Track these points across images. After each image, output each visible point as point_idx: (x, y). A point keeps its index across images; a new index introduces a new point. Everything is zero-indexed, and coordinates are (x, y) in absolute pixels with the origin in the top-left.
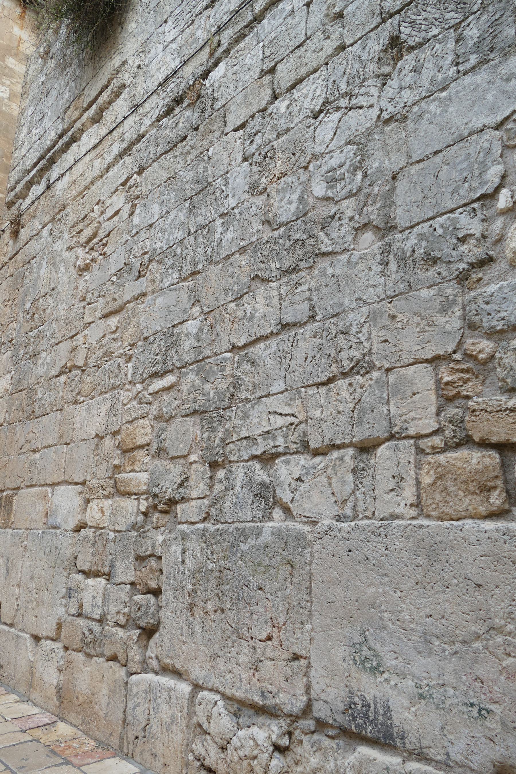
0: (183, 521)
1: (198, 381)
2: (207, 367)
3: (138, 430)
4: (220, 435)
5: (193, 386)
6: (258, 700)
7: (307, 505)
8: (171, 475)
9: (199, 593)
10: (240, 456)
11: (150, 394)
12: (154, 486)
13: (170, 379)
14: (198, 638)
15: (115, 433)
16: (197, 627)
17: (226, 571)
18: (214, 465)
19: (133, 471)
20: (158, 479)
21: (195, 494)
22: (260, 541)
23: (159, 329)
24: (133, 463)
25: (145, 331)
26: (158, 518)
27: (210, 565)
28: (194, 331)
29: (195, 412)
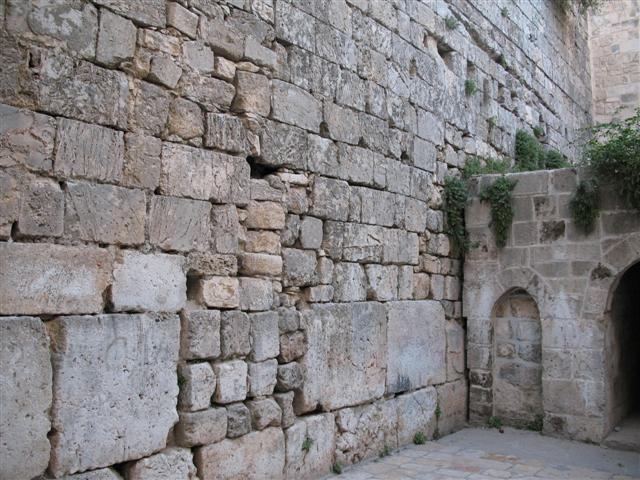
1: (328, 193)
2: (335, 185)
3: (271, 213)
4: (341, 240)
5: (324, 194)
6: (368, 398)
7: (383, 292)
8: (307, 264)
12: (292, 270)
13: (301, 178)
14: (335, 380)
15: (241, 207)
16: (335, 372)
18: (335, 261)
19: (265, 252)
21: (325, 281)
22: (368, 312)
24: (264, 245)
25: (277, 112)
28: (325, 148)
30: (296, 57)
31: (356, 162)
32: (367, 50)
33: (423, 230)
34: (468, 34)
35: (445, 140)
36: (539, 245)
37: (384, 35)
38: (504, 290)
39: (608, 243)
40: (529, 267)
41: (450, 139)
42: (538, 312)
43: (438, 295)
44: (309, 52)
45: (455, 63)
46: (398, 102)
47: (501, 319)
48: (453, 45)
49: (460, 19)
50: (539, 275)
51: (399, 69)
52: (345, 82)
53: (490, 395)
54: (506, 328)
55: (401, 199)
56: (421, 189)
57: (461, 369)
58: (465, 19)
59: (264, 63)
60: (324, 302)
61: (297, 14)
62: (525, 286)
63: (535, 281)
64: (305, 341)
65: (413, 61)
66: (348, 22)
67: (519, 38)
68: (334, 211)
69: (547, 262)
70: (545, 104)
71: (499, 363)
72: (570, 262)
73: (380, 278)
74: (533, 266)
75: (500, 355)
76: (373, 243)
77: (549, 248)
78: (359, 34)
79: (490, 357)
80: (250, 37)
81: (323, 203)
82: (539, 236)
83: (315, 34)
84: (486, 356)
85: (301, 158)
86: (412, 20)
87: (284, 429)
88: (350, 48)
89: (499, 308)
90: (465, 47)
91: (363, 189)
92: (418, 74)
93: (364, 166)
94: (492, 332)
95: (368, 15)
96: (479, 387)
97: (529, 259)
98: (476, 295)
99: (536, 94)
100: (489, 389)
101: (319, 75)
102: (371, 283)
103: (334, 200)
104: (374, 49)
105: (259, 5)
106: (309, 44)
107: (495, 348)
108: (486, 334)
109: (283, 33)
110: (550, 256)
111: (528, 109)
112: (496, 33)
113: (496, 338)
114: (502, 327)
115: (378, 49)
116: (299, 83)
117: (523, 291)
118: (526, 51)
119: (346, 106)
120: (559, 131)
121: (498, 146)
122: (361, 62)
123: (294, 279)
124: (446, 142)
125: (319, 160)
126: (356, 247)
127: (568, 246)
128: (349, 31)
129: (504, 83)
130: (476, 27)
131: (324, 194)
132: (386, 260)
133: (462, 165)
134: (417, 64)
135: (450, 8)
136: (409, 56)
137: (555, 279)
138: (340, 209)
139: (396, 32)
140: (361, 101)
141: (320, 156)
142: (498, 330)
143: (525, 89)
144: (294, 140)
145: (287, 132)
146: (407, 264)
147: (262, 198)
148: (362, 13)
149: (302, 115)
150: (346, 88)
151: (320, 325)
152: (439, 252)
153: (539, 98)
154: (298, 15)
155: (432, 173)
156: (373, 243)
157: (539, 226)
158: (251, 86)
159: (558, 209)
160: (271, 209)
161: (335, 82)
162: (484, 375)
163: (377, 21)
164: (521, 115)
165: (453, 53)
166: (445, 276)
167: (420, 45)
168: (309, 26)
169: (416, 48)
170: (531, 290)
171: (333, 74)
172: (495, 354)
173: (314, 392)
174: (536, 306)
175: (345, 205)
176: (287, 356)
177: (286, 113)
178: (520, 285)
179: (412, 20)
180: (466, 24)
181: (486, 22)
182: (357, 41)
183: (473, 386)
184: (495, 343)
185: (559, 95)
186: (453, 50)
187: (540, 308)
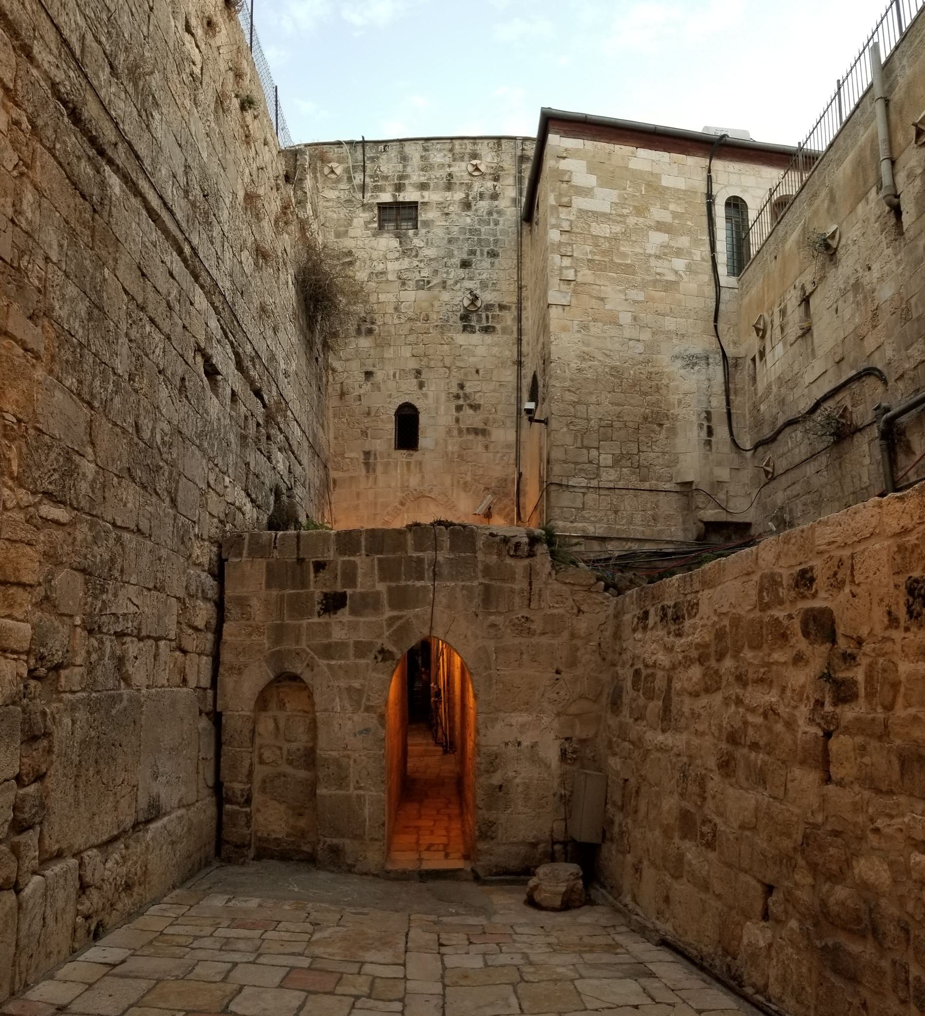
0: (67, 689)
1: (89, 538)
3: (24, 560)
5: (85, 539)
6: (115, 833)
9: (83, 763)
10: (109, 630)
11: (41, 517)
13: (60, 514)
17: (102, 736)
20: (47, 636)
23: (58, 436)
24: (11, 606)
26: (35, 687)
27: (93, 734)
28: (90, 477)
29: (83, 571)
30: (66, 347)
31: (121, 500)
32: (140, 353)
33: (182, 596)
34: (233, 357)
35: (208, 483)
36: (316, 619)
37: (157, 339)
38: (272, 677)
39: (392, 620)
40: (304, 645)
41: (212, 482)
42: (313, 704)
43: (192, 683)
44: (80, 343)
45: (220, 390)
46: (167, 428)
47: (263, 714)
48: (220, 367)
49: (227, 337)
50: (316, 657)
51: (169, 387)
52: (116, 392)
53: (249, 816)
54: (271, 725)
55: (164, 553)
56: (183, 543)
57: (211, 782)
58: (231, 338)
59: (30, 346)
60: (74, 692)
61: (70, 288)
62: (299, 672)
63: (310, 666)
64: (50, 751)
65: (183, 379)
66: (123, 314)
67: (275, 371)
68: (94, 563)
69: (326, 641)
70: (293, 453)
71: (260, 772)
72: (351, 642)
73: (136, 658)
74: (308, 646)
75: (262, 762)
76: (133, 609)
77: (327, 624)
78: (134, 334)
79: (251, 765)
80: (15, 306)
81: (84, 550)
82: (317, 608)
83: (89, 320)
84: (246, 763)
85: (64, 487)
86: (184, 327)
87: (18, 892)
88: (123, 347)
89: (262, 702)
90: (230, 371)
91: (126, 536)
92: (186, 397)
93: (130, 505)
94: (253, 731)
95: (142, 309)
96: (236, 807)
97: (304, 638)
98: (236, 682)
99: (287, 439)
100: (248, 809)
101: (89, 377)
102: (127, 664)
103: (96, 548)
104: (147, 355)
105: (29, 263)
106: (81, 331)
107: (256, 752)
108: (246, 732)
109: (53, 309)
110: (329, 635)
111: (280, 456)
112: (257, 361)
113: (258, 741)
114: (266, 726)
115: (151, 356)
116: (68, 384)
117: (295, 678)
118: (280, 388)
119: (115, 424)
120: (304, 485)
121: (254, 496)
122: (133, 369)
123: (42, 658)
124: (209, 486)
125: (83, 492)
126: (114, 614)
127: (350, 622)
128: (124, 326)
129: (261, 422)
130: (241, 351)
131: (85, 539)
132: (144, 633)
133: (222, 516)
134: (187, 383)
135: (218, 320)
136: (180, 372)
137: (333, 662)
138: (101, 562)
139: (169, 338)
140: (130, 420)
141: (84, 487)
142: (261, 728)
143: (278, 433)
144: (58, 461)
145: (50, 448)
146: (165, 639)
147: (15, 538)
148: (138, 306)
149: (69, 427)
150: (117, 400)
151: (70, 724)
152: (196, 624)
153: (290, 445)
154: (72, 290)
155: (194, 522)
156: (133, 609)
157: (318, 596)
158: (13, 376)
159: (339, 577)
160: (24, 555)
161: (106, 389)
162: (242, 790)
163: (152, 321)
164: (274, 462)
165: (219, 377)
166: (199, 654)
167: (190, 361)
168: (82, 308)
169: (187, 363)
170: (307, 676)
171: (105, 380)
172: (256, 760)
173: (56, 828)
174: (310, 696)
175: (106, 557)
176: (27, 775)
177: (51, 421)
178: (294, 671)
179: (184, 327)
180: (232, 344)
181: (249, 346)
182: (131, 341)
183: (228, 807)
184: (257, 745)
185: (305, 444)
186: (219, 373)
187: (317, 698)
